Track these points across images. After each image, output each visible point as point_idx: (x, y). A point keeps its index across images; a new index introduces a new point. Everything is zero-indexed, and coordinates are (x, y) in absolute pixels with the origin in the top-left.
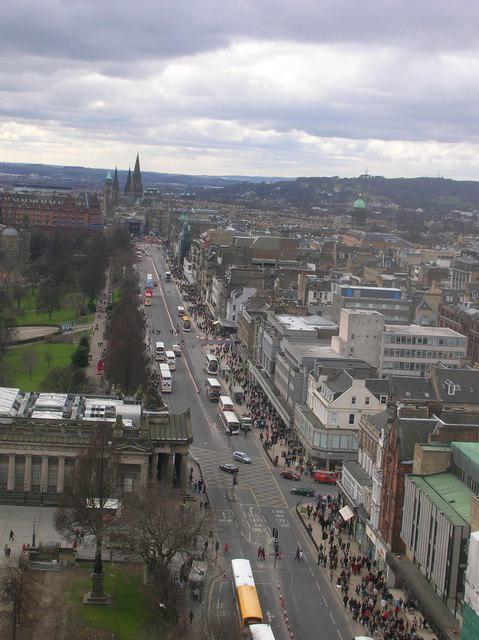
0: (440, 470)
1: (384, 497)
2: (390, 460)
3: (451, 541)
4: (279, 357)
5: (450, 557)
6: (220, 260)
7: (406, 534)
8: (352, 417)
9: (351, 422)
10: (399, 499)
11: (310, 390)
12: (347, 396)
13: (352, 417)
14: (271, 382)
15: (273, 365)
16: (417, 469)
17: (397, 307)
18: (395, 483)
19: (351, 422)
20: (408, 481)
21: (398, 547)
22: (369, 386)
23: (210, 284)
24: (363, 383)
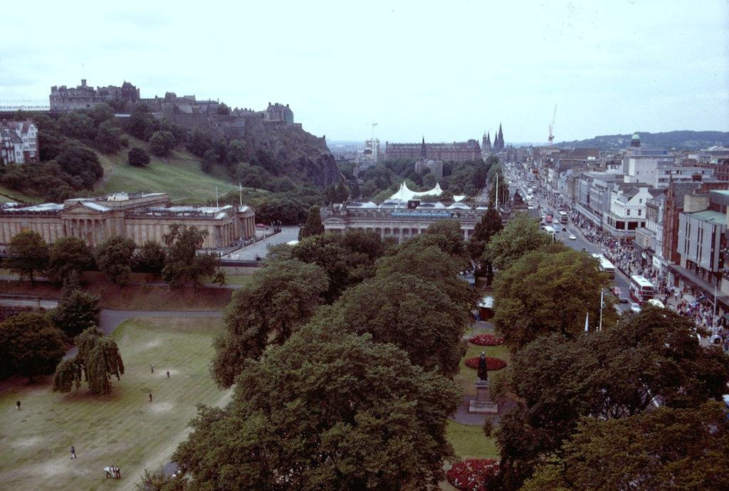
0: (703, 209)
1: (665, 234)
2: (668, 209)
3: (714, 235)
4: (592, 190)
5: (713, 246)
6: (552, 160)
7: (681, 249)
8: (640, 211)
9: (640, 214)
10: (675, 230)
11: (612, 202)
12: (635, 199)
13: (640, 211)
14: (588, 208)
15: (588, 196)
16: (686, 209)
17: (666, 160)
18: (672, 221)
19: (640, 214)
20: (681, 216)
21: (676, 258)
22: (649, 191)
23: (547, 175)
24: (646, 189)
